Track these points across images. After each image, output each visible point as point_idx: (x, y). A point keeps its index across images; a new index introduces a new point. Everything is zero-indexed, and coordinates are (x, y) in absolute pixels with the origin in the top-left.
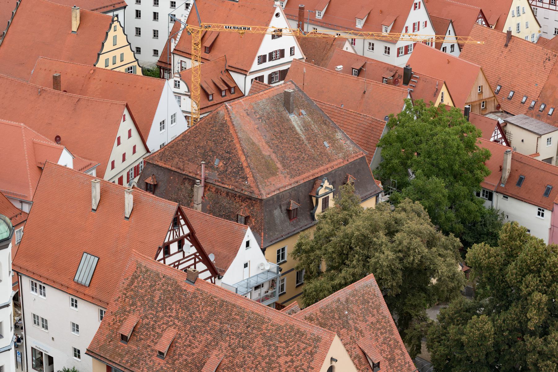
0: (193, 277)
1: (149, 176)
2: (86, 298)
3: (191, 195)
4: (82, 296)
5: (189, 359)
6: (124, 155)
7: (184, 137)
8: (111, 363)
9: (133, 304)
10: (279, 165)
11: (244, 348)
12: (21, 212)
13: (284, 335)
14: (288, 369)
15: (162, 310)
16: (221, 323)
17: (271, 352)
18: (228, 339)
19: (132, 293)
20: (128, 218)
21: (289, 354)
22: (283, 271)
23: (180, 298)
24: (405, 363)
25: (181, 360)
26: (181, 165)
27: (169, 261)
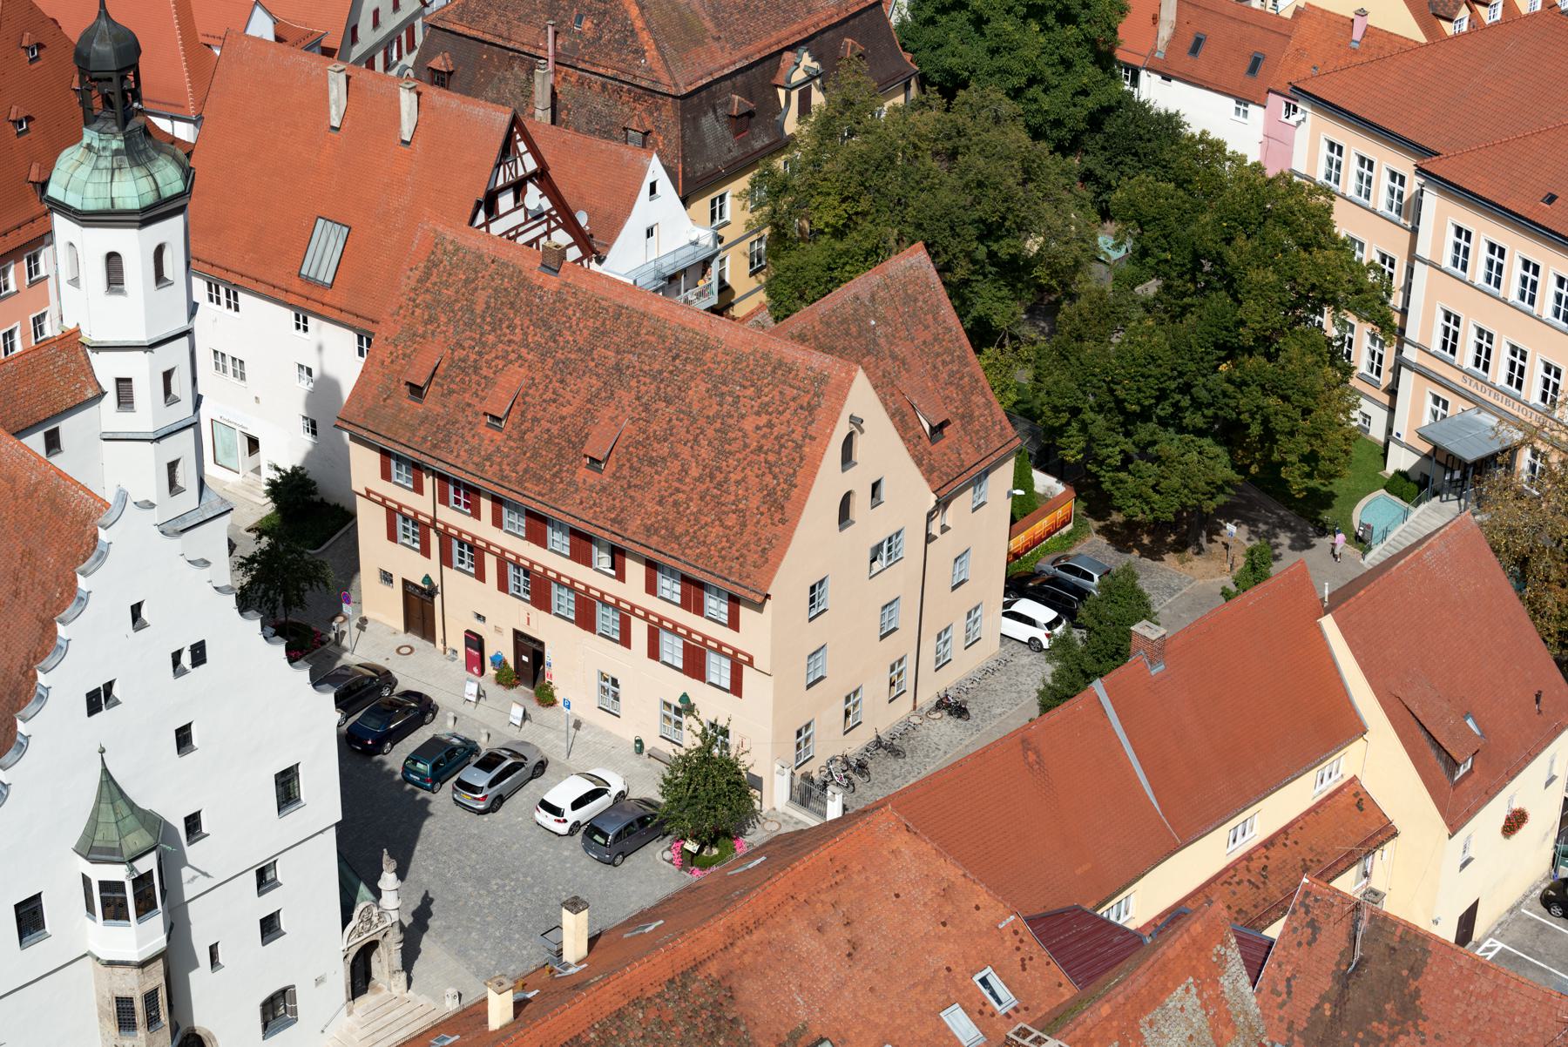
0: (554, 261)
1: (436, 53)
2: (327, 311)
3: (528, 94)
4: (317, 307)
5: (555, 430)
8: (390, 443)
9: (430, 321)
10: (709, 24)
11: (668, 402)
12: (174, 141)
13: (752, 372)
14: (763, 442)
15: (494, 330)
16: (618, 352)
17: (726, 408)
18: (634, 383)
19: (428, 297)
20: (408, 143)
21: (763, 409)
22: (726, 242)
24: (994, 424)
25: (538, 430)
26: (502, 28)
27: (497, 228)
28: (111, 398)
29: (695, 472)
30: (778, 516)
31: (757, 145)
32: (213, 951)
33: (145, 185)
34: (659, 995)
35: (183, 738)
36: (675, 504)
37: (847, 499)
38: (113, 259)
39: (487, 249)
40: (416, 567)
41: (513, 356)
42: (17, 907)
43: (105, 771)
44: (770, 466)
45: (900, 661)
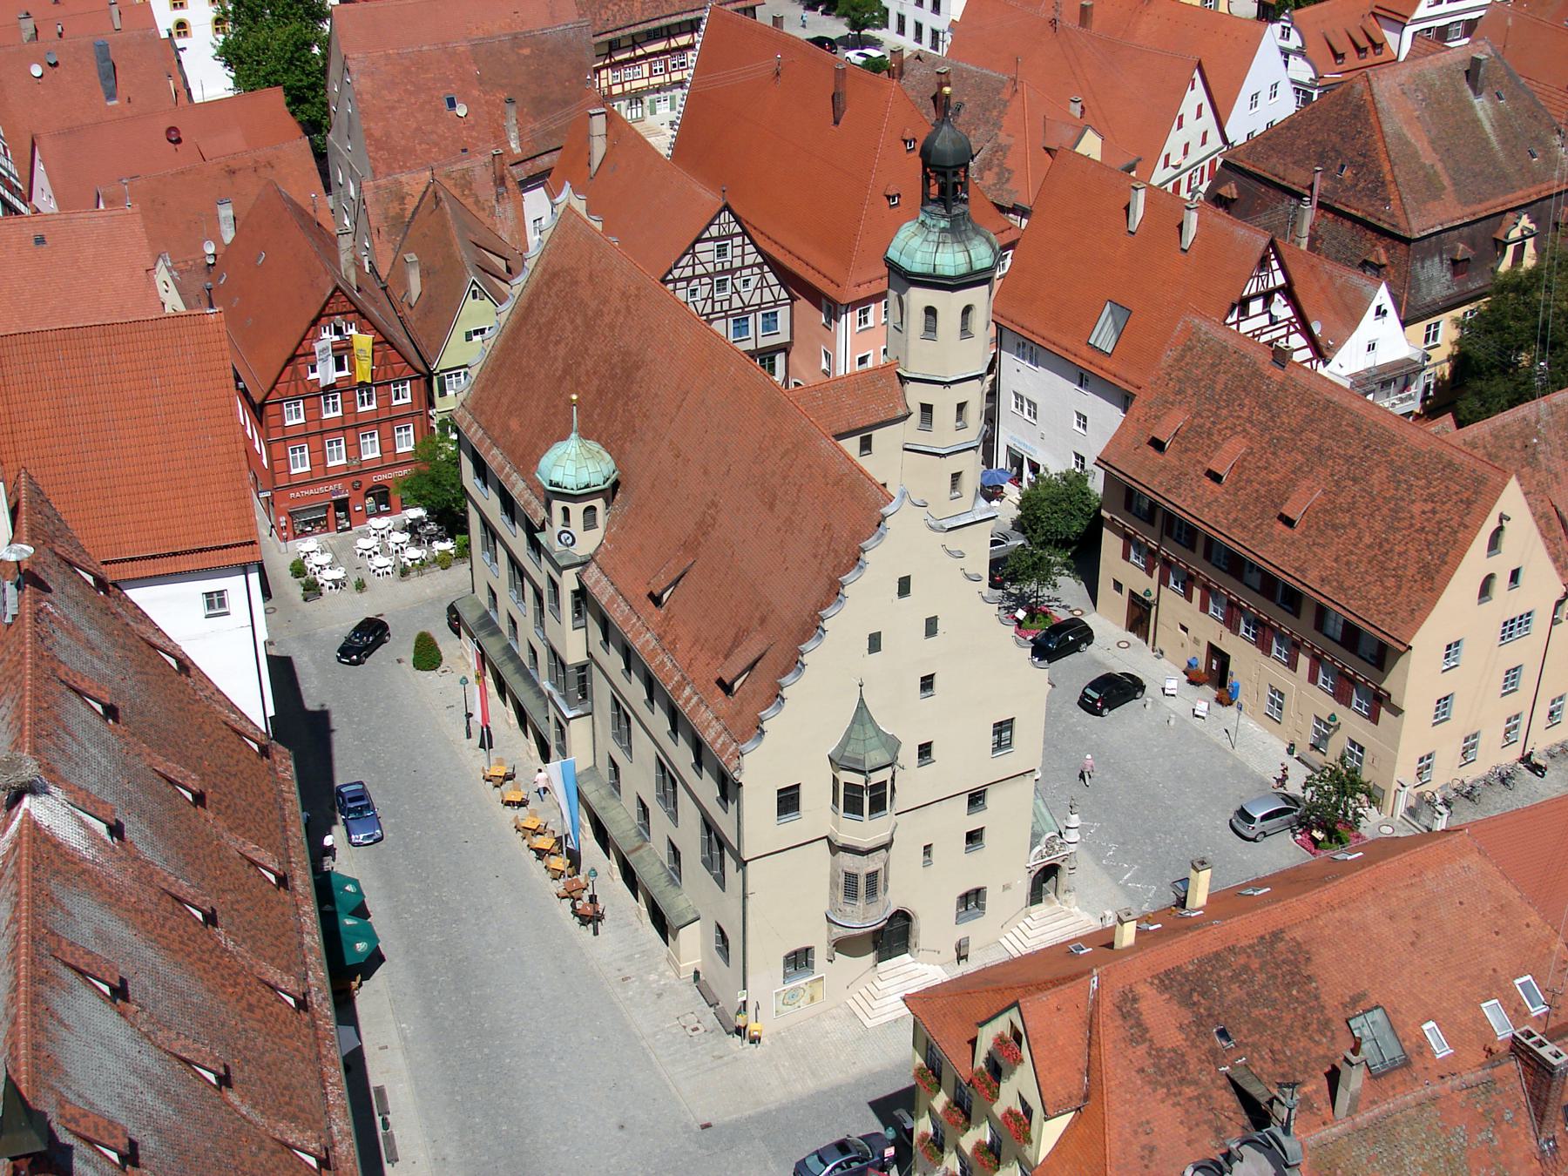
0: (1281, 356)
1: (1226, 182)
3: (1294, 223)
5: (1263, 491)
6: (1187, 145)
7: (1289, 123)
9: (1179, 392)
10: (1446, 181)
11: (1355, 480)
18: (1330, 463)
19: (1181, 373)
21: (1430, 498)
23: (1258, 389)
26: (1280, 170)
27: (1246, 327)
28: (916, 417)
29: (1368, 540)
30: (1428, 585)
31: (1471, 286)
32: (927, 849)
33: (961, 258)
34: (1251, 946)
35: (927, 683)
36: (1348, 563)
37: (1490, 577)
38: (931, 311)
39: (1232, 342)
40: (1141, 581)
41: (1239, 429)
42: (779, 792)
43: (861, 699)
44: (1429, 544)
45: (1517, 717)
